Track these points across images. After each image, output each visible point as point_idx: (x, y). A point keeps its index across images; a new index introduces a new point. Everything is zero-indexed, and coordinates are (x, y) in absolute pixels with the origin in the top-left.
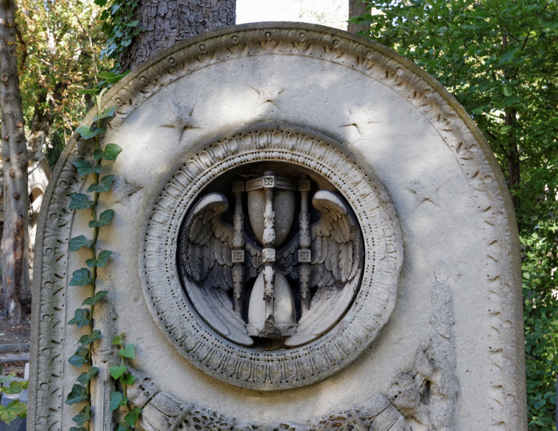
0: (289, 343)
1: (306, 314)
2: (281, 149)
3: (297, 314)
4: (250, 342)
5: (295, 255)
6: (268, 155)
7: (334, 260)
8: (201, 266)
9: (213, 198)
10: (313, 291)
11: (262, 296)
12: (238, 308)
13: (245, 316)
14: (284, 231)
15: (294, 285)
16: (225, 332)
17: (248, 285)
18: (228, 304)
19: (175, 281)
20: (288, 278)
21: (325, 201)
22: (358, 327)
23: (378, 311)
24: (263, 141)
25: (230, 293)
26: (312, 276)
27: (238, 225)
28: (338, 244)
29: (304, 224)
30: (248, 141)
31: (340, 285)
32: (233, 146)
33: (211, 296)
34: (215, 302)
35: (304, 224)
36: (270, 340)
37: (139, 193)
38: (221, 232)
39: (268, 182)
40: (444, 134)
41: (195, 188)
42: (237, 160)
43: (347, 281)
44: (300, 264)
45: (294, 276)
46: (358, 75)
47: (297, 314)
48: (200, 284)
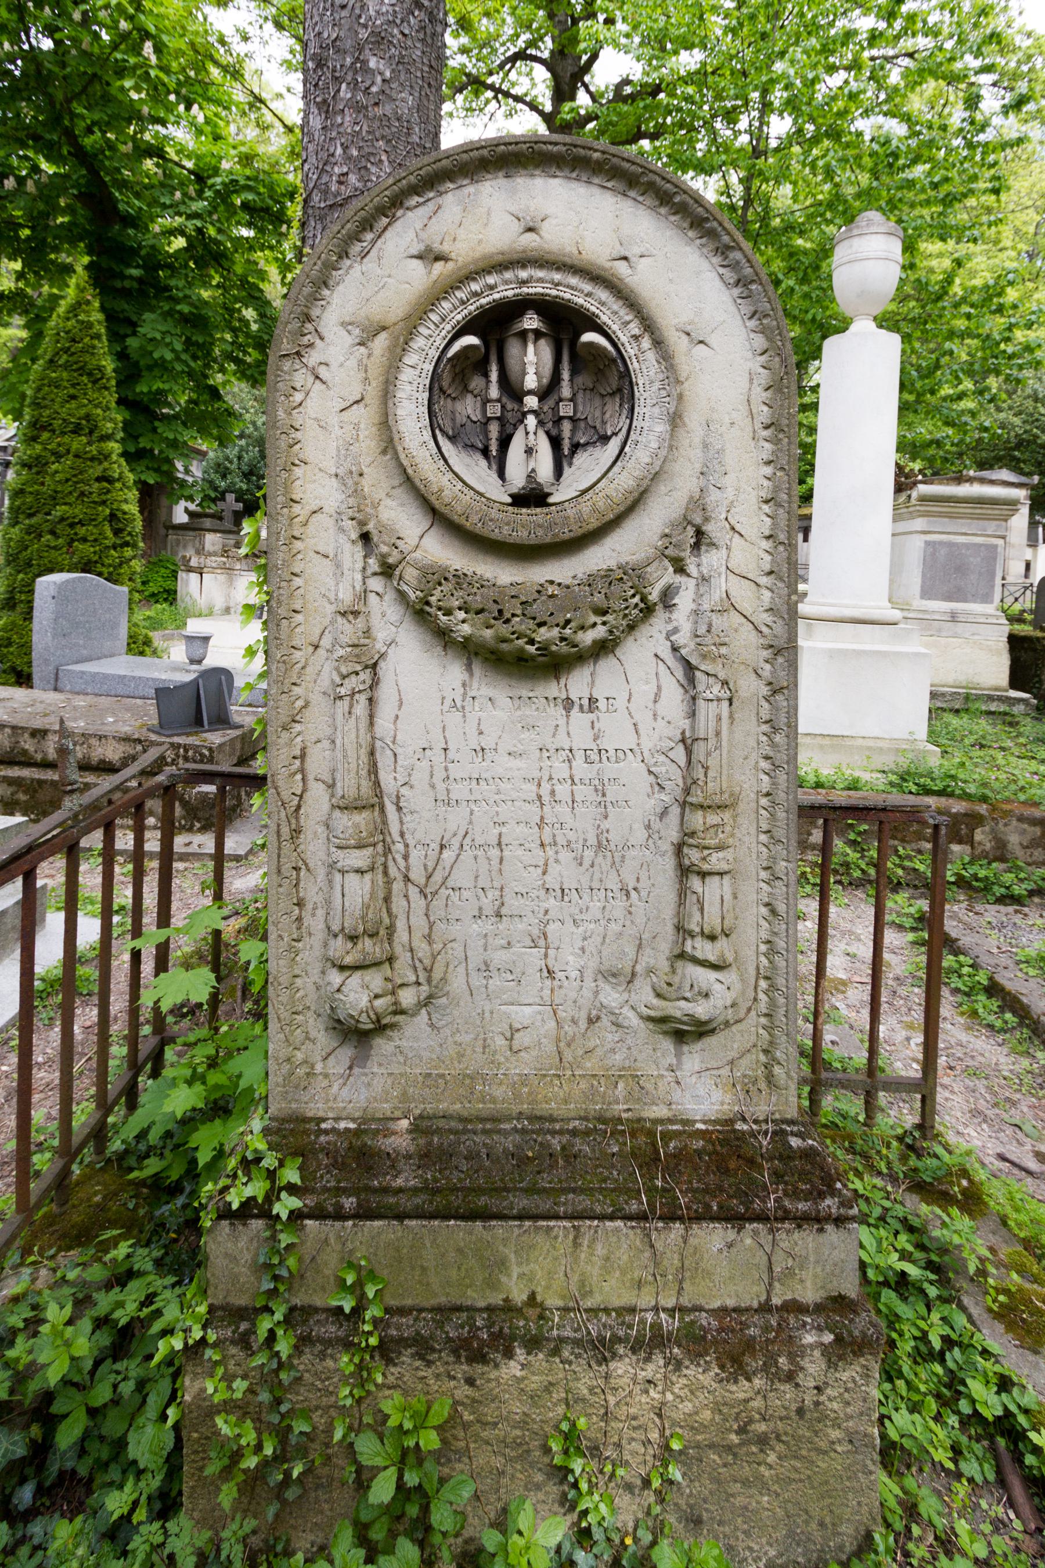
0: (551, 500)
1: (567, 471)
2: (542, 284)
3: (558, 472)
4: (509, 500)
5: (555, 409)
6: (531, 291)
7: (598, 414)
8: (453, 420)
9: (471, 340)
10: (576, 447)
11: (523, 448)
12: (494, 467)
13: (501, 474)
14: (545, 381)
15: (555, 442)
16: (482, 490)
17: (505, 442)
18: (483, 463)
19: (427, 435)
20: (547, 433)
21: (591, 344)
22: (624, 480)
23: (648, 460)
24: (523, 274)
25: (485, 452)
26: (573, 431)
27: (494, 376)
28: (603, 396)
29: (566, 375)
30: (508, 275)
31: (605, 439)
32: (491, 280)
33: (463, 455)
34: (468, 460)
35: (566, 375)
36: (532, 497)
37: (383, 335)
38: (476, 382)
39: (531, 322)
40: (721, 270)
41: (448, 327)
42: (496, 296)
43: (615, 434)
44: (562, 418)
45: (554, 432)
46: (630, 203)
47: (558, 472)
48: (452, 439)
